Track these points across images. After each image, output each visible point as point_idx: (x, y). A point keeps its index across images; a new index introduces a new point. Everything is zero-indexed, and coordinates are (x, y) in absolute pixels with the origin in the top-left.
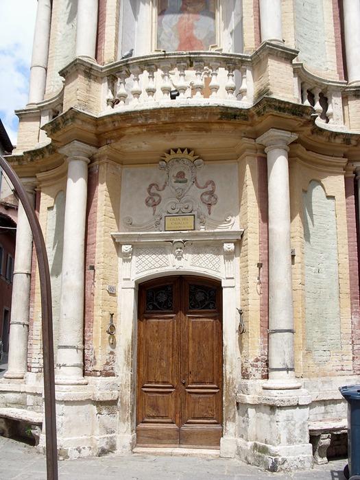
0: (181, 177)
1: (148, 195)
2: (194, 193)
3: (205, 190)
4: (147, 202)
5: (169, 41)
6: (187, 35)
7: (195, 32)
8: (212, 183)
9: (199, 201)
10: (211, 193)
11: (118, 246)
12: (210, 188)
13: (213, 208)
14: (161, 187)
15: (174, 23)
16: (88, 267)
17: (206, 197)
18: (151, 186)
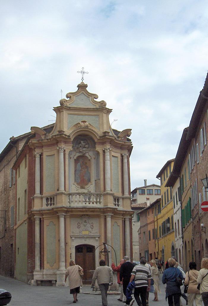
0: (85, 222)
1: (77, 225)
2: (88, 225)
3: (91, 225)
4: (77, 227)
5: (77, 179)
6: (83, 178)
7: (85, 177)
8: (92, 223)
9: (90, 228)
10: (93, 226)
11: (71, 237)
12: (92, 225)
13: (93, 229)
14: (80, 224)
15: (79, 174)
16: (66, 244)
17: (91, 227)
18: (78, 223)
